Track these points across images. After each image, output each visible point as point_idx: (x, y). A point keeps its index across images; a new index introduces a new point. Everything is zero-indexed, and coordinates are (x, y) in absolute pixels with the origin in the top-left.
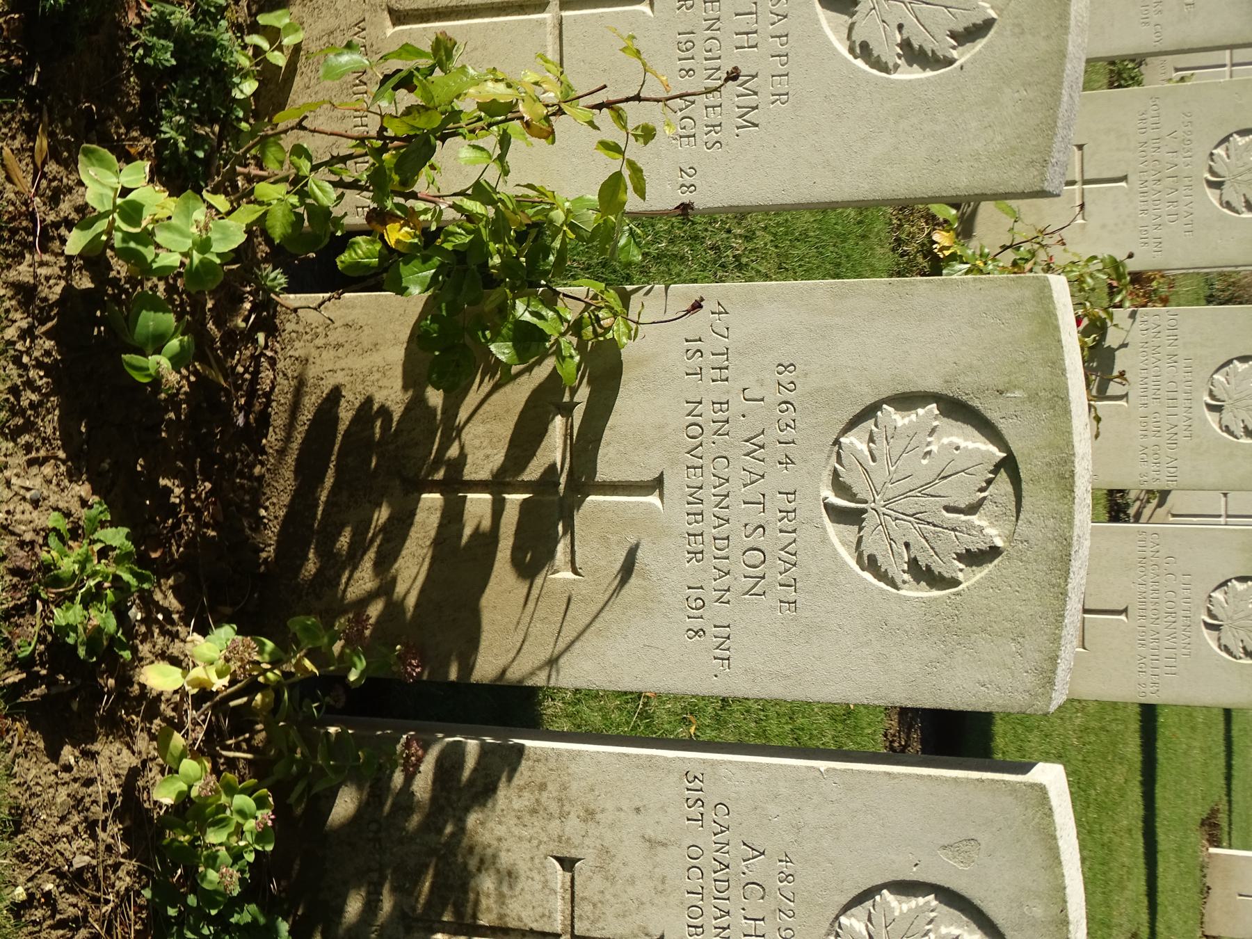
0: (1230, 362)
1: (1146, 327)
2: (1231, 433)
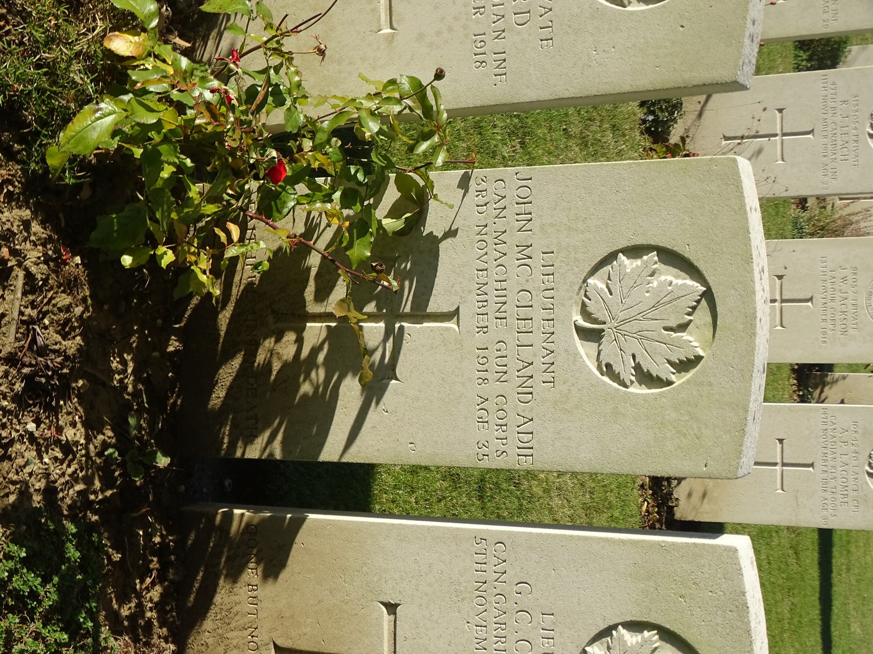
0: (611, 258)
1: (486, 200)
2: (616, 377)
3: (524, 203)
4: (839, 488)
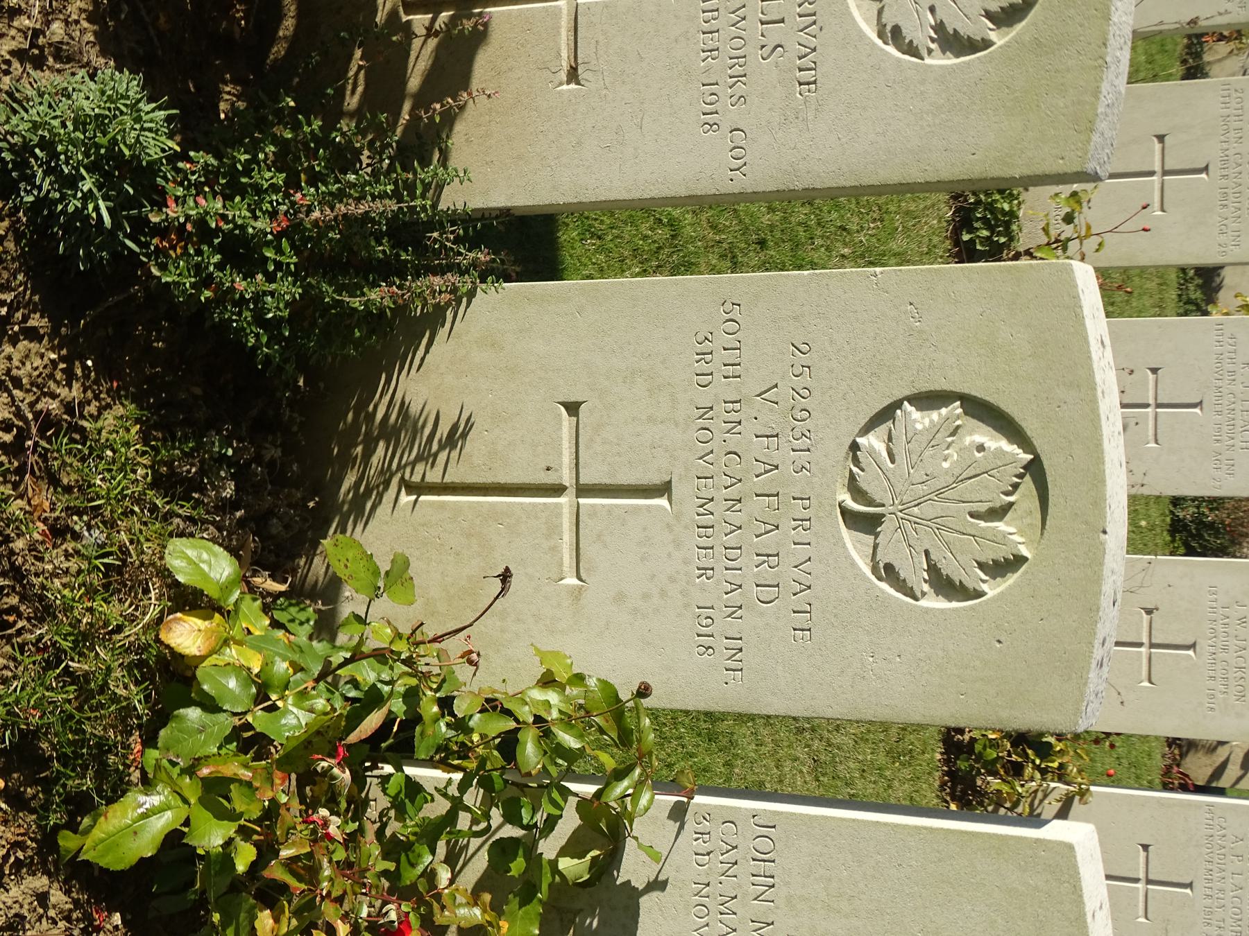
3: (764, 861)
4: (1229, 921)
